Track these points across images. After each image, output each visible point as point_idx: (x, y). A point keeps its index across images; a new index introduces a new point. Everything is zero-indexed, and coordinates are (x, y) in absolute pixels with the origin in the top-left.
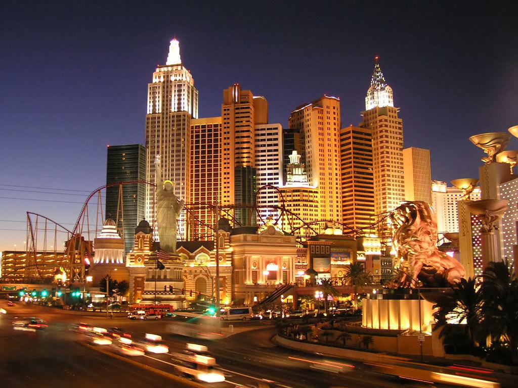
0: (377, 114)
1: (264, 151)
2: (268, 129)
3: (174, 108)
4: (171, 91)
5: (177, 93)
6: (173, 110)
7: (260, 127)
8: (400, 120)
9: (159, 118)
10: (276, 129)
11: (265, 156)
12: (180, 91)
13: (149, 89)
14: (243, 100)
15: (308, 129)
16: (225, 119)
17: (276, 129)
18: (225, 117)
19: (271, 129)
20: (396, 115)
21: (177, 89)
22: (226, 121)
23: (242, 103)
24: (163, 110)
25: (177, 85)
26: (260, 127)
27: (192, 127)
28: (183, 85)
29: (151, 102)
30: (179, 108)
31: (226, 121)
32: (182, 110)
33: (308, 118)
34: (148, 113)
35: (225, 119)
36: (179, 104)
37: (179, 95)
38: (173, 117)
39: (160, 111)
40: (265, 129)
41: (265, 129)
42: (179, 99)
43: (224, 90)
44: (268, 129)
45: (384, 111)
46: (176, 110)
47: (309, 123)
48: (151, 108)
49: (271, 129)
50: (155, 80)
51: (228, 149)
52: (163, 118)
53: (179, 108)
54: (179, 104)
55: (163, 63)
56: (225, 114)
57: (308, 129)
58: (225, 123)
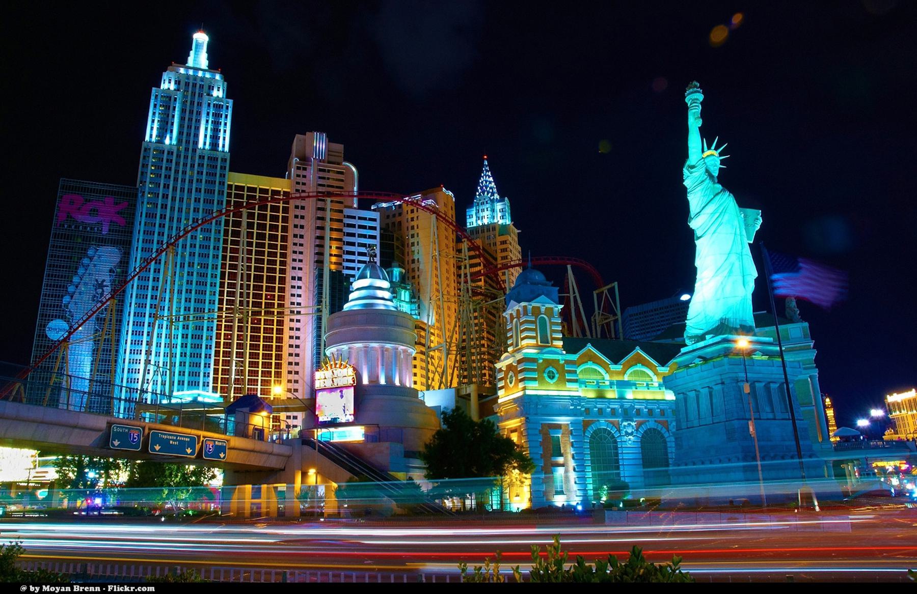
0: (497, 232)
1: (353, 253)
2: (360, 218)
3: (203, 141)
4: (199, 113)
5: (211, 119)
6: (201, 145)
7: (347, 212)
8: (519, 248)
9: (170, 153)
10: (375, 220)
11: (353, 261)
12: (217, 116)
13: (153, 98)
14: (332, 159)
15: (411, 232)
16: (298, 183)
17: (375, 220)
18: (299, 180)
19: (365, 219)
20: (516, 239)
21: (212, 111)
22: (300, 187)
23: (329, 162)
24: (179, 141)
25: (212, 105)
26: (347, 212)
27: (230, 187)
28: (224, 108)
29: (156, 121)
30: (214, 145)
31: (300, 187)
32: (220, 148)
33: (410, 216)
34: (147, 138)
35: (298, 183)
36: (215, 138)
37: (216, 124)
38: (202, 157)
39: (174, 142)
40: (354, 217)
41: (354, 217)
42: (216, 131)
43: (298, 137)
44: (360, 218)
45: (504, 229)
46: (207, 147)
47: (414, 223)
48: (155, 133)
49: (365, 219)
50: (168, 84)
51: (302, 237)
52: (178, 156)
53: (214, 145)
54: (215, 138)
55: (183, 61)
56: (298, 176)
57: (411, 232)
58: (297, 190)
